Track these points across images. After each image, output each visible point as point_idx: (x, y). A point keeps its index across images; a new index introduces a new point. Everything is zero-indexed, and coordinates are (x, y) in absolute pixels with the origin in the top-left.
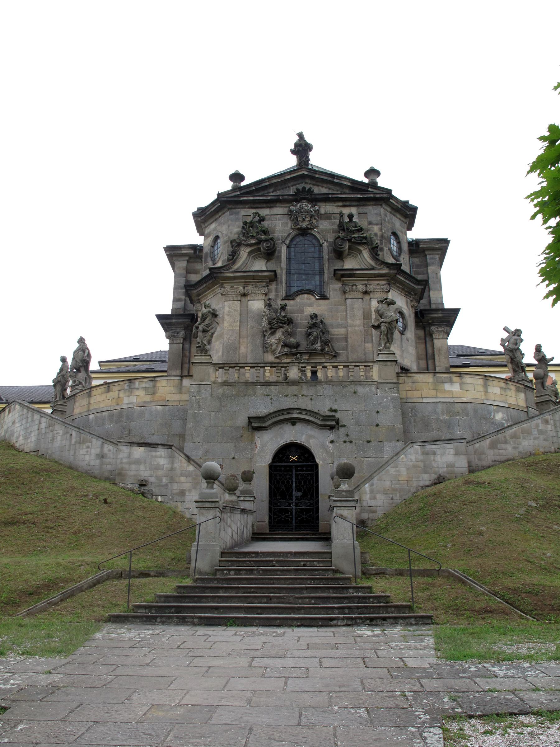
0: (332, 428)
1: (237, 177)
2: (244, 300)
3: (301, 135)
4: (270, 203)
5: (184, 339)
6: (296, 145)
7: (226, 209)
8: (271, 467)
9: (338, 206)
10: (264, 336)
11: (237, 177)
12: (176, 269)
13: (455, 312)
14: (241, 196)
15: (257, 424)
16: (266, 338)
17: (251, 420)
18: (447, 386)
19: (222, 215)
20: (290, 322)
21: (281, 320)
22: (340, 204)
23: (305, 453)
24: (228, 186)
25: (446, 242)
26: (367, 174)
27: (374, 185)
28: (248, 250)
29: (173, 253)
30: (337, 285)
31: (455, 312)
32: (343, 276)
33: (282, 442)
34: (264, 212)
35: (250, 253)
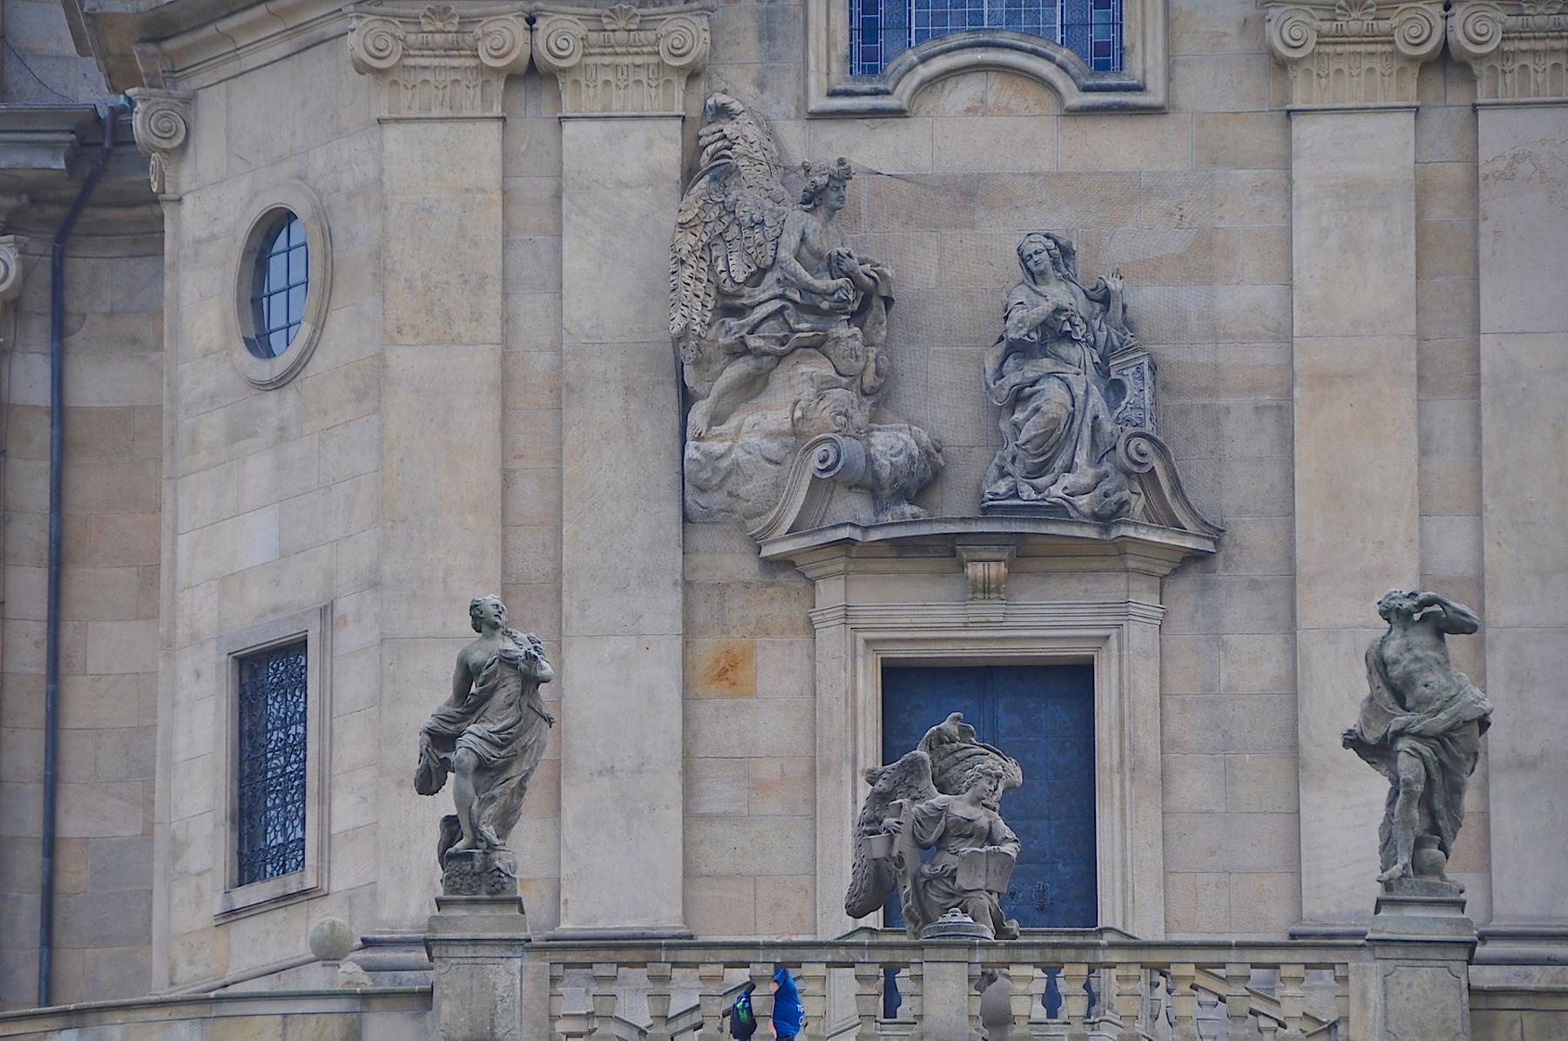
2: (533, 113)
10: (686, 399)
16: (698, 416)
20: (869, 300)
21: (806, 290)
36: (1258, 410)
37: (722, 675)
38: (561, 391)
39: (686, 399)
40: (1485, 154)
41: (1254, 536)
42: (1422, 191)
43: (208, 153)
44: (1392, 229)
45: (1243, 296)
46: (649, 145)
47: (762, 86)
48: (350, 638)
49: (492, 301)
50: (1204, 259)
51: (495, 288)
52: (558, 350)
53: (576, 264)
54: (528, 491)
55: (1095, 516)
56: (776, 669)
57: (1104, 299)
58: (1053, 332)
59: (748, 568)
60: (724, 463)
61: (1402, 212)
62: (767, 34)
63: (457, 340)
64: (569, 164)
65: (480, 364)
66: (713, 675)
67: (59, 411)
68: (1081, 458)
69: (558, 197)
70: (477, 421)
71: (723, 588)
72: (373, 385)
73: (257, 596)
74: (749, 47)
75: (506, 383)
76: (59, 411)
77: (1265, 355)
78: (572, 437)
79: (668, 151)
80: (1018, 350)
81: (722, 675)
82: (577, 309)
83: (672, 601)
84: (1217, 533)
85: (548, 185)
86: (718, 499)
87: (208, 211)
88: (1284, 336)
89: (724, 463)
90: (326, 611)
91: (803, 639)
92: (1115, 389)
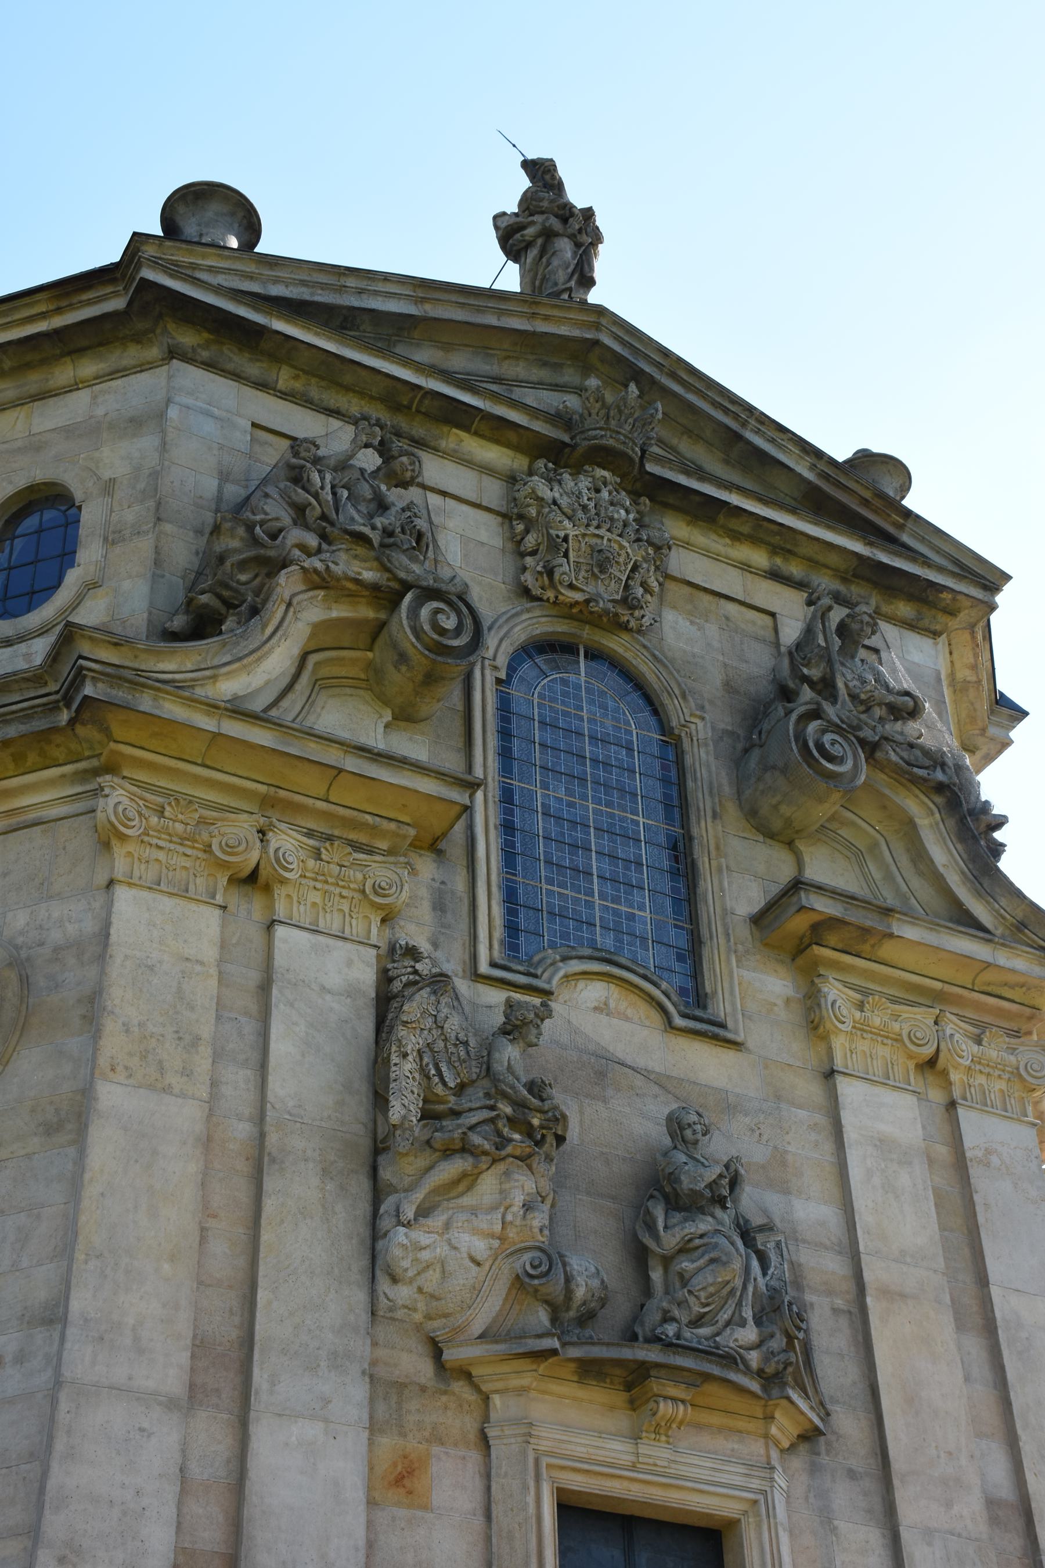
2: (250, 909)
3: (541, 173)
7: (154, 352)
9: (745, 567)
19: (100, 378)
22: (760, 558)
36: (835, 1311)
37: (399, 1481)
39: (378, 1193)
40: (968, 1142)
41: (849, 1425)
46: (349, 963)
47: (435, 945)
49: (203, 1063)
51: (205, 1051)
52: (260, 1118)
53: (280, 1047)
55: (760, 1373)
59: (422, 1368)
60: (425, 1255)
63: (167, 1090)
64: (280, 960)
65: (184, 1115)
66: (399, 1482)
68: (748, 1313)
69: (265, 988)
70: (180, 1167)
71: (401, 1386)
75: (207, 1142)
78: (270, 1205)
81: (399, 1481)
82: (279, 1087)
83: (360, 1391)
85: (254, 977)
86: (403, 1293)
89: (425, 1255)
91: (474, 1456)
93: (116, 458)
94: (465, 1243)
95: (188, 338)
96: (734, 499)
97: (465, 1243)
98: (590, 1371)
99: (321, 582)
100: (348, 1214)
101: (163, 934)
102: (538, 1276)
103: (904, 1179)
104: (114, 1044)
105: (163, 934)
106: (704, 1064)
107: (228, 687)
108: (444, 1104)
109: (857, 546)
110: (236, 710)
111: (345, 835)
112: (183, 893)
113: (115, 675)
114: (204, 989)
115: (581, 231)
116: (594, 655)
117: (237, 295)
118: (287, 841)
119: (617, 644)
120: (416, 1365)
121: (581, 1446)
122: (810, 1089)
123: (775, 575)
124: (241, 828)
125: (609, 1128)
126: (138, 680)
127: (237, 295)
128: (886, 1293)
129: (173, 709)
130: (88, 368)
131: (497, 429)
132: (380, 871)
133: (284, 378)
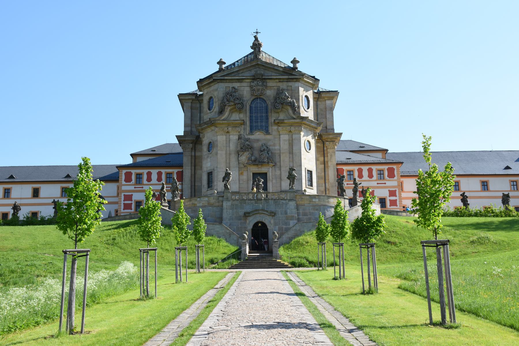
0: (273, 216)
1: (221, 63)
2: (228, 134)
4: (240, 81)
5: (192, 149)
6: (253, 44)
8: (253, 230)
11: (221, 63)
12: (185, 107)
13: (340, 134)
14: (224, 74)
15: (247, 215)
17: (245, 213)
18: (314, 200)
20: (251, 148)
22: (278, 81)
23: (264, 225)
24: (216, 68)
25: (336, 93)
26: (292, 62)
27: (295, 68)
28: (229, 108)
29: (182, 97)
30: (275, 128)
31: (340, 134)
32: (278, 123)
33: (256, 221)
34: (236, 85)
35: (231, 110)
38: (230, 154)
41: (278, 164)
42: (289, 140)
43: (205, 138)
44: (287, 143)
45: (277, 147)
48: (215, 171)
50: (274, 145)
53: (231, 145)
54: (228, 161)
56: (245, 173)
57: (267, 148)
58: (264, 150)
59: (243, 166)
61: (288, 142)
62: (244, 129)
65: (224, 152)
66: (241, 174)
67: (195, 156)
72: (217, 154)
73: (209, 169)
74: (243, 130)
75: (226, 153)
76: (195, 156)
77: (278, 151)
79: (237, 138)
80: (261, 151)
82: (231, 148)
83: (238, 169)
84: (276, 164)
87: (205, 141)
88: (280, 150)
90: (214, 169)
92: (268, 154)
93: (216, 94)
94: (244, 158)
95: (219, 81)
96: (272, 77)
97: (244, 158)
98: (254, 165)
99: (229, 106)
100: (236, 157)
101: (221, 139)
102: (249, 159)
103: (286, 143)
104: (219, 148)
105: (221, 139)
106: (268, 137)
107: (223, 118)
108: (245, 146)
109: (287, 77)
110: (223, 120)
111: (235, 126)
112: (222, 135)
113: (214, 120)
114: (225, 142)
115: (260, 45)
116: (260, 98)
117: (221, 76)
118: (230, 129)
119: (262, 97)
120: (242, 166)
121: (254, 170)
122: (278, 136)
123: (280, 82)
124: (226, 128)
125: (256, 145)
126: (215, 120)
127: (221, 76)
128: (283, 153)
129: (219, 122)
130: (213, 84)
131: (248, 79)
132: (237, 128)
133: (228, 81)
